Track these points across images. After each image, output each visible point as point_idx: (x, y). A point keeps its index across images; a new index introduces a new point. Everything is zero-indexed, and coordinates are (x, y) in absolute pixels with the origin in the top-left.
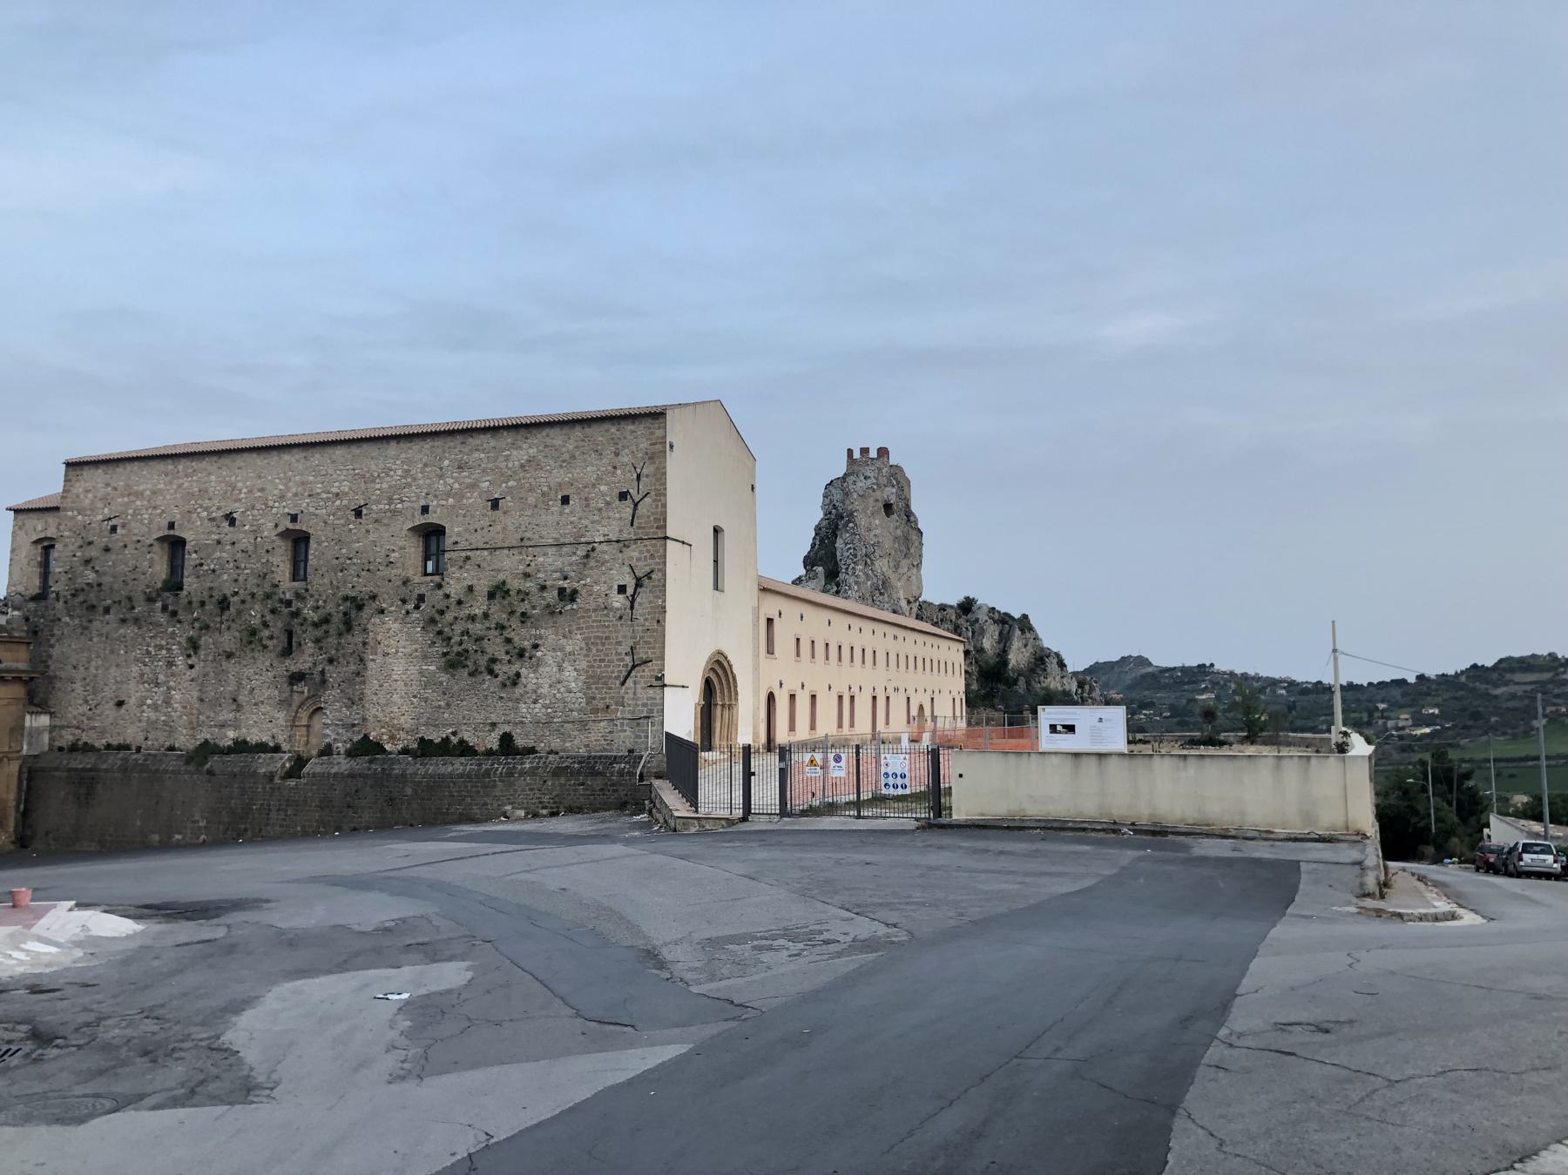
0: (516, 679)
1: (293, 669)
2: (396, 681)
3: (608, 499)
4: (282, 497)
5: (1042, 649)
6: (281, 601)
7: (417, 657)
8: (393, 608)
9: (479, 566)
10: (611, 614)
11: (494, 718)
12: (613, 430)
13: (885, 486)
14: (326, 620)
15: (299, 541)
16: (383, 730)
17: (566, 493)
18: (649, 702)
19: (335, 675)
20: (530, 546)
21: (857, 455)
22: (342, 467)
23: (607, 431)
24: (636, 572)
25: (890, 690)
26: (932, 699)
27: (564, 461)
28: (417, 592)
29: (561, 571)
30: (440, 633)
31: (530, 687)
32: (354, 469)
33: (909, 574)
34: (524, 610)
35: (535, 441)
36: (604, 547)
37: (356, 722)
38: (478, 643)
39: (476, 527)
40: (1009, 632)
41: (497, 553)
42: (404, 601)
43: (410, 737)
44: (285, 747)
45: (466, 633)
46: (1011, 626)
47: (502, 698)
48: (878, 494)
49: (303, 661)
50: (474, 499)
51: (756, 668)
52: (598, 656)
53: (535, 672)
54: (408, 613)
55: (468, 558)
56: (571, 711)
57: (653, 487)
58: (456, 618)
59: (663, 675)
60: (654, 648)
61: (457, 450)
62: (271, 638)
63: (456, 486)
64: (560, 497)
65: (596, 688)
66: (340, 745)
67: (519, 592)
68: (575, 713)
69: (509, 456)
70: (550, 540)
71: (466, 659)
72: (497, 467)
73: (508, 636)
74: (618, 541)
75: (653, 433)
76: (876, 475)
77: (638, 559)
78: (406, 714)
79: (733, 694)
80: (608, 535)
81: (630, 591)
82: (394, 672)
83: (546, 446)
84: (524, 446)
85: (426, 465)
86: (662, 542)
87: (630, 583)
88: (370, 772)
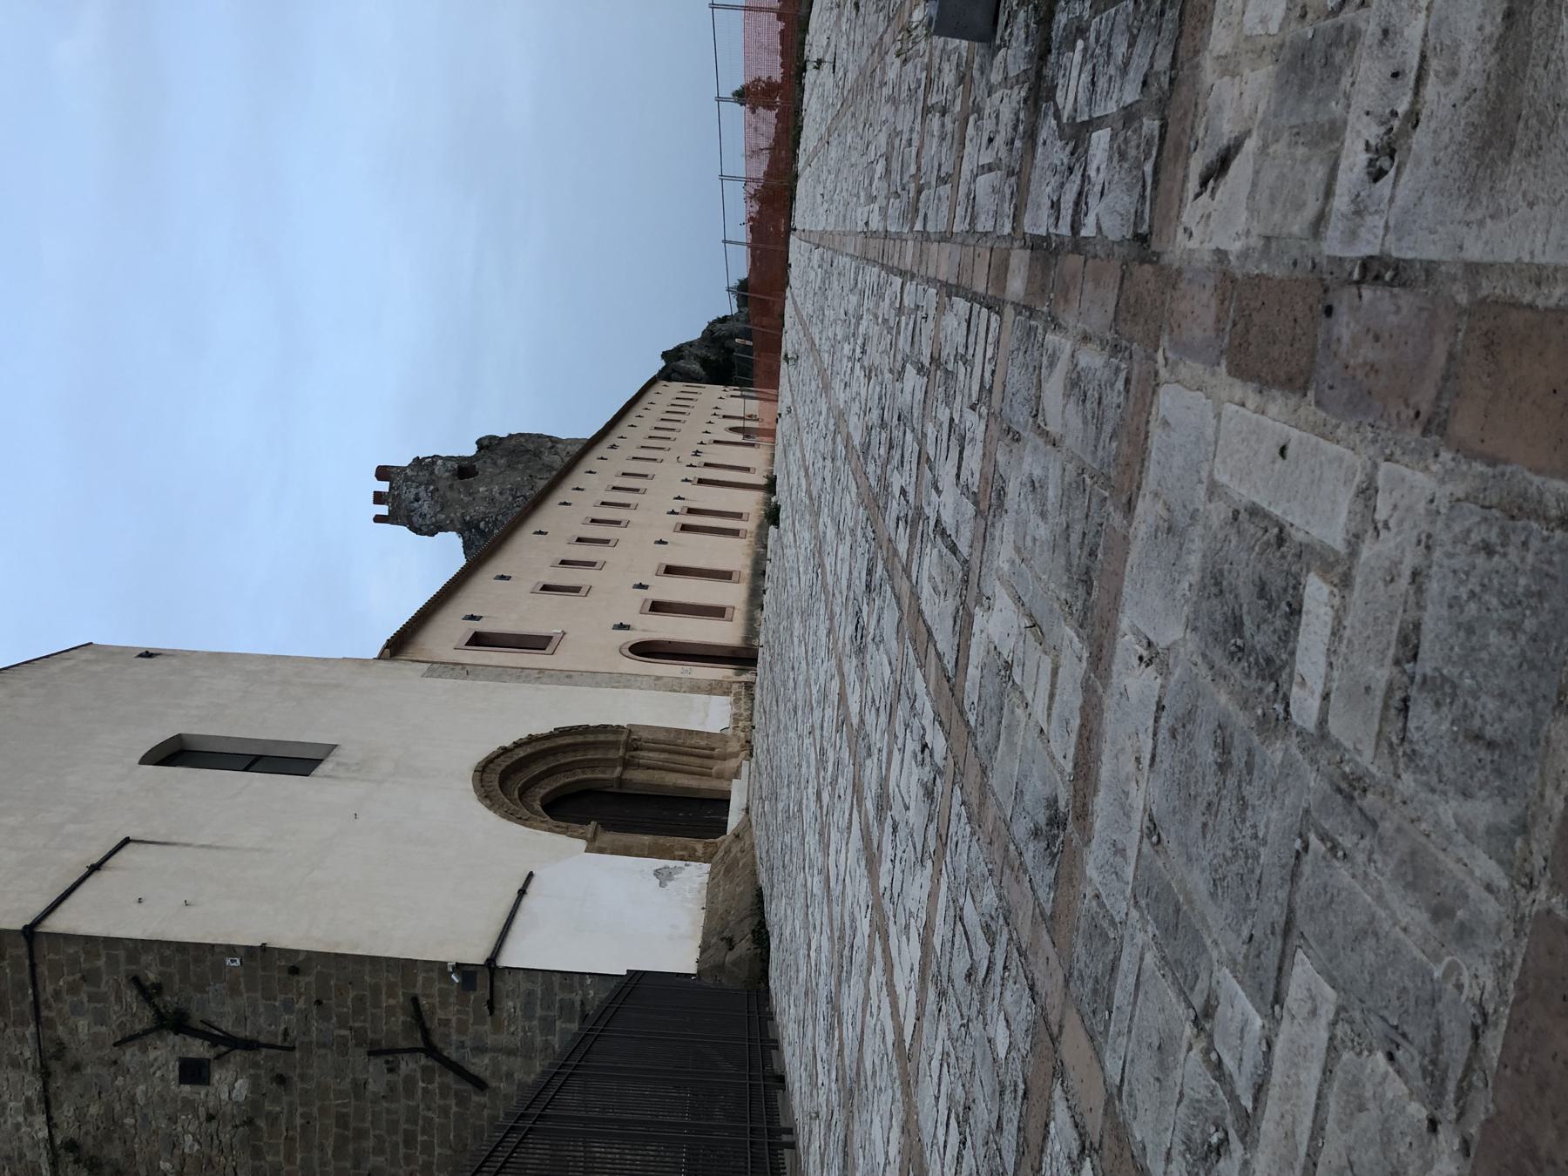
5: (703, 338)
10: (268, 1107)
13: (432, 473)
18: (539, 1012)
21: (383, 510)
24: (138, 1028)
25: (695, 461)
26: (724, 417)
46: (674, 371)
51: (568, 677)
52: (395, 1146)
60: (376, 989)
74: (46, 1075)
77: (100, 1018)
79: (602, 737)
80: (28, 1101)
81: (198, 1049)
87: (166, 1052)
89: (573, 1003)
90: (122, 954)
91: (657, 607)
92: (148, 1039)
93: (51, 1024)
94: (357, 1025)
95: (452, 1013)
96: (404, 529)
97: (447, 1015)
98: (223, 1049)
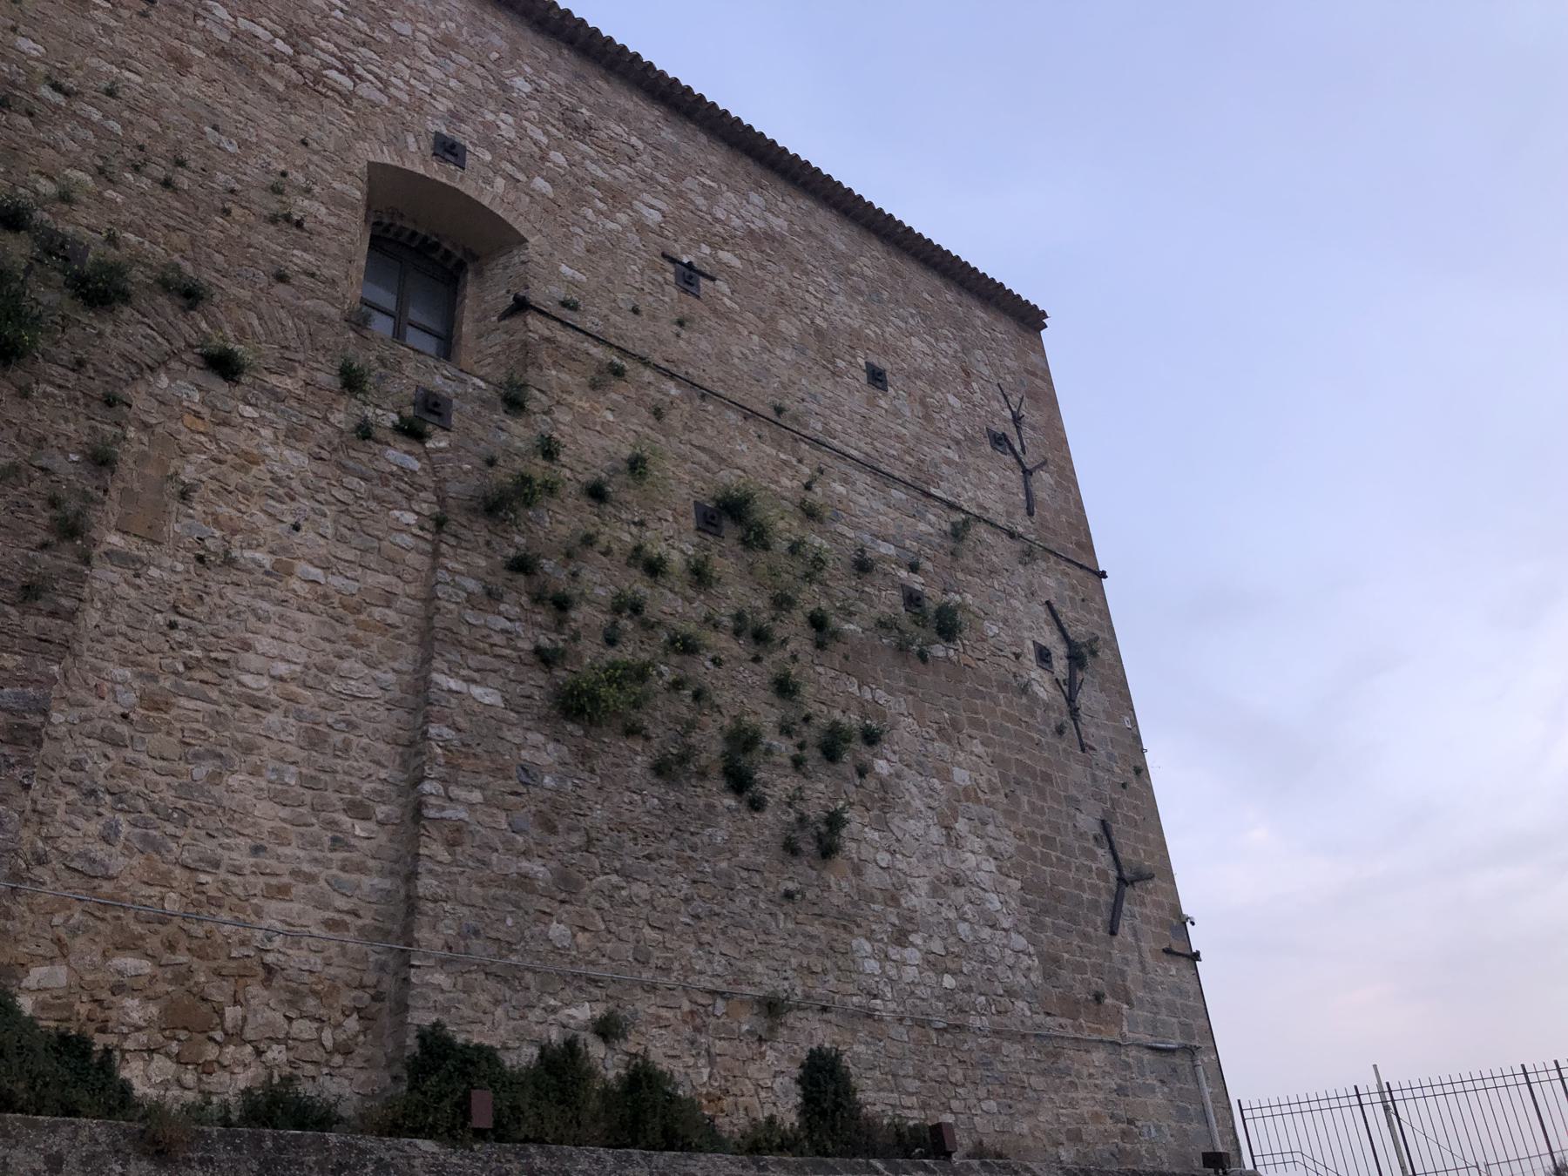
11: (767, 981)
16: (129, 963)
30: (522, 565)
42: (352, 381)
43: (304, 1028)
54: (365, 432)
55: (618, 372)
78: (299, 889)
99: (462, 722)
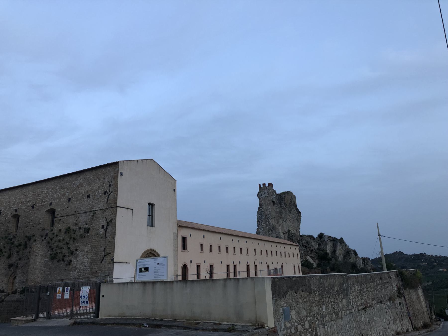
0: (70, 263)
1: (10, 262)
2: (37, 265)
3: (101, 195)
4: (14, 204)
5: (348, 249)
6: (9, 239)
7: (44, 256)
8: (39, 239)
9: (63, 222)
10: (99, 236)
11: (63, 278)
12: (103, 170)
13: (272, 195)
14: (20, 245)
15: (17, 217)
17: (89, 194)
19: (21, 264)
20: (78, 214)
21: (262, 186)
22: (30, 192)
23: (102, 171)
24: (107, 220)
27: (89, 183)
28: (46, 233)
29: (85, 222)
30: (50, 247)
31: (74, 265)
32: (33, 193)
33: (283, 224)
34: (74, 237)
35: (82, 177)
36: (99, 212)
37: (24, 281)
38: (61, 250)
39: (64, 208)
40: (336, 244)
41: (69, 217)
42: (42, 236)
44: (5, 291)
45: (57, 246)
47: (66, 270)
48: (269, 198)
49: (13, 260)
50: (64, 199)
53: (76, 259)
55: (61, 220)
56: (85, 274)
57: (114, 189)
58: (55, 241)
59: (114, 258)
61: (61, 183)
62: (5, 252)
63: (60, 195)
64: (87, 195)
65: (93, 265)
66: (19, 289)
67: (73, 230)
68: (86, 275)
69: (74, 183)
70: (83, 211)
71: (57, 256)
72: (71, 187)
73: (69, 247)
74: (103, 209)
75: (115, 170)
76: (268, 192)
77: (108, 215)
80: (100, 207)
81: (105, 227)
82: (37, 262)
83: (85, 178)
84: (79, 179)
85: (52, 189)
86: (115, 208)
87: (105, 223)
88: (22, 299)
89: (110, 273)
90: (115, 217)
91: (198, 267)
92: (106, 221)
93: (108, 210)
94: (108, 246)
95: (109, 258)
96: (258, 191)
97: (107, 259)
98: (105, 230)
99: (46, 263)
